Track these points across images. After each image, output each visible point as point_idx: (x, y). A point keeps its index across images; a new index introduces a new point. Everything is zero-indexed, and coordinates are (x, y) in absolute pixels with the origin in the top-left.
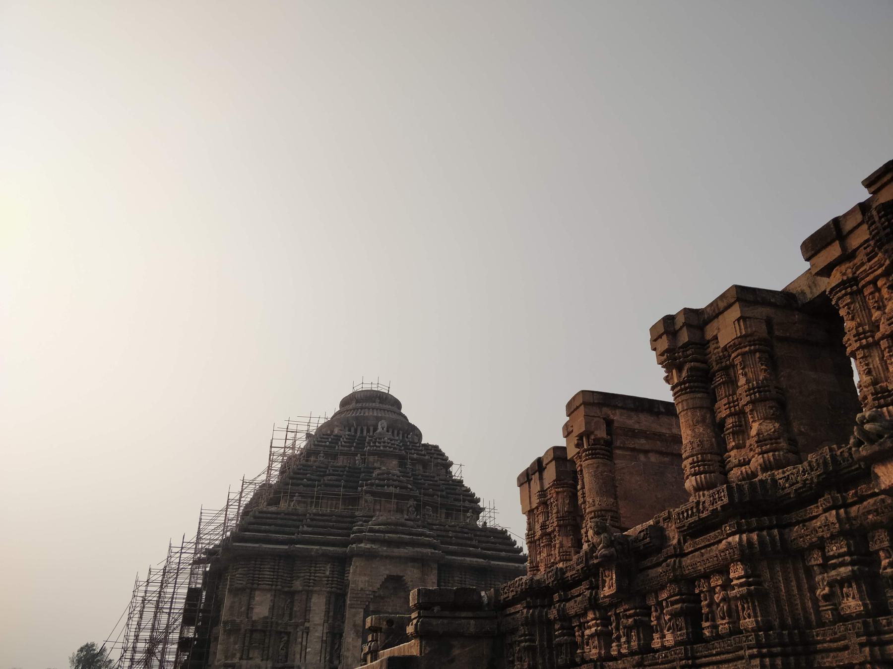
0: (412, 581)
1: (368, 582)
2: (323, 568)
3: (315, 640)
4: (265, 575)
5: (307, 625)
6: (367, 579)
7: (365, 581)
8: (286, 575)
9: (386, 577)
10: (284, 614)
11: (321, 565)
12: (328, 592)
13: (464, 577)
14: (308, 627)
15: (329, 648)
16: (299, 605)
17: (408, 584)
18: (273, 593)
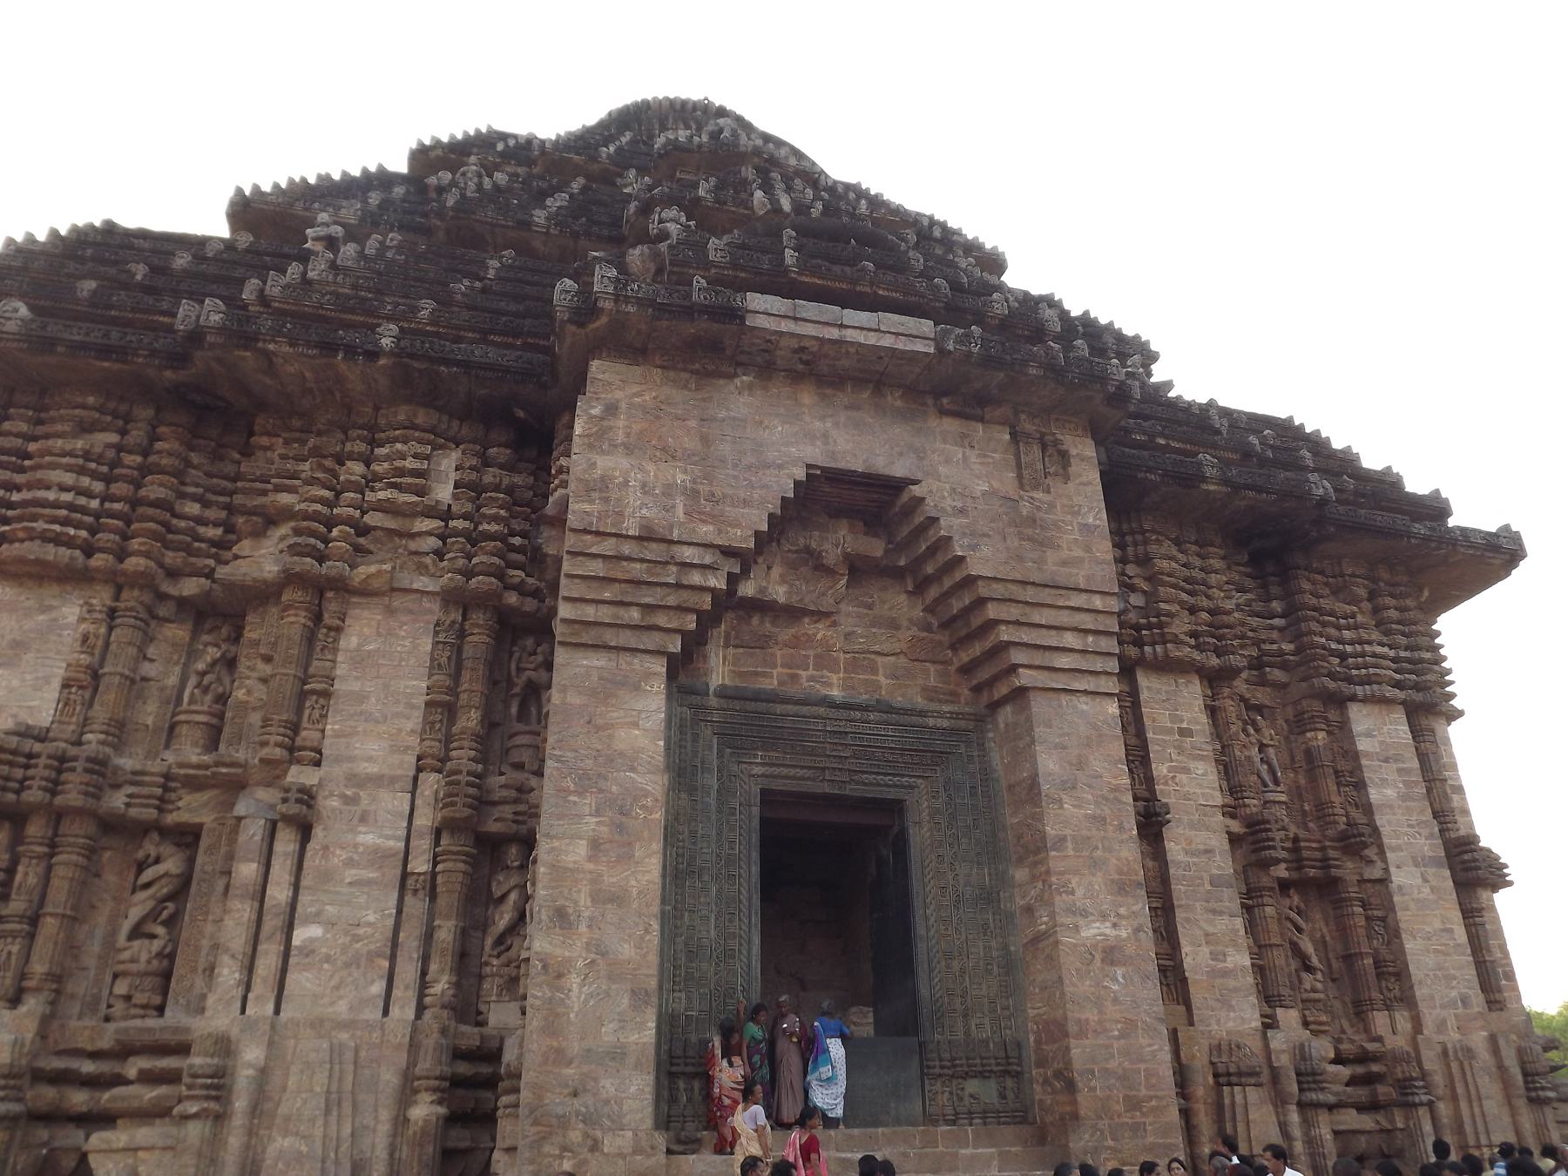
0: (962, 512)
1: (695, 494)
2: (410, 463)
3: (351, 874)
4: (48, 488)
5: (298, 775)
6: (680, 477)
7: (669, 490)
8: (193, 508)
9: (801, 474)
10: (172, 727)
11: (399, 446)
12: (449, 598)
13: (1197, 562)
14: (307, 796)
15: (451, 923)
16: (267, 669)
17: (942, 522)
18: (102, 597)
